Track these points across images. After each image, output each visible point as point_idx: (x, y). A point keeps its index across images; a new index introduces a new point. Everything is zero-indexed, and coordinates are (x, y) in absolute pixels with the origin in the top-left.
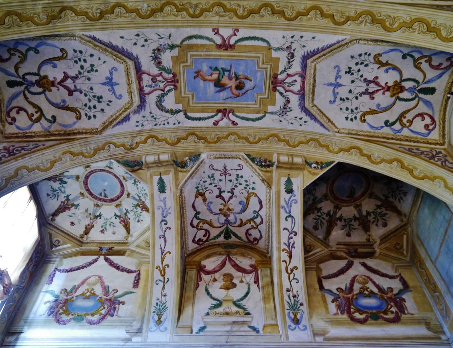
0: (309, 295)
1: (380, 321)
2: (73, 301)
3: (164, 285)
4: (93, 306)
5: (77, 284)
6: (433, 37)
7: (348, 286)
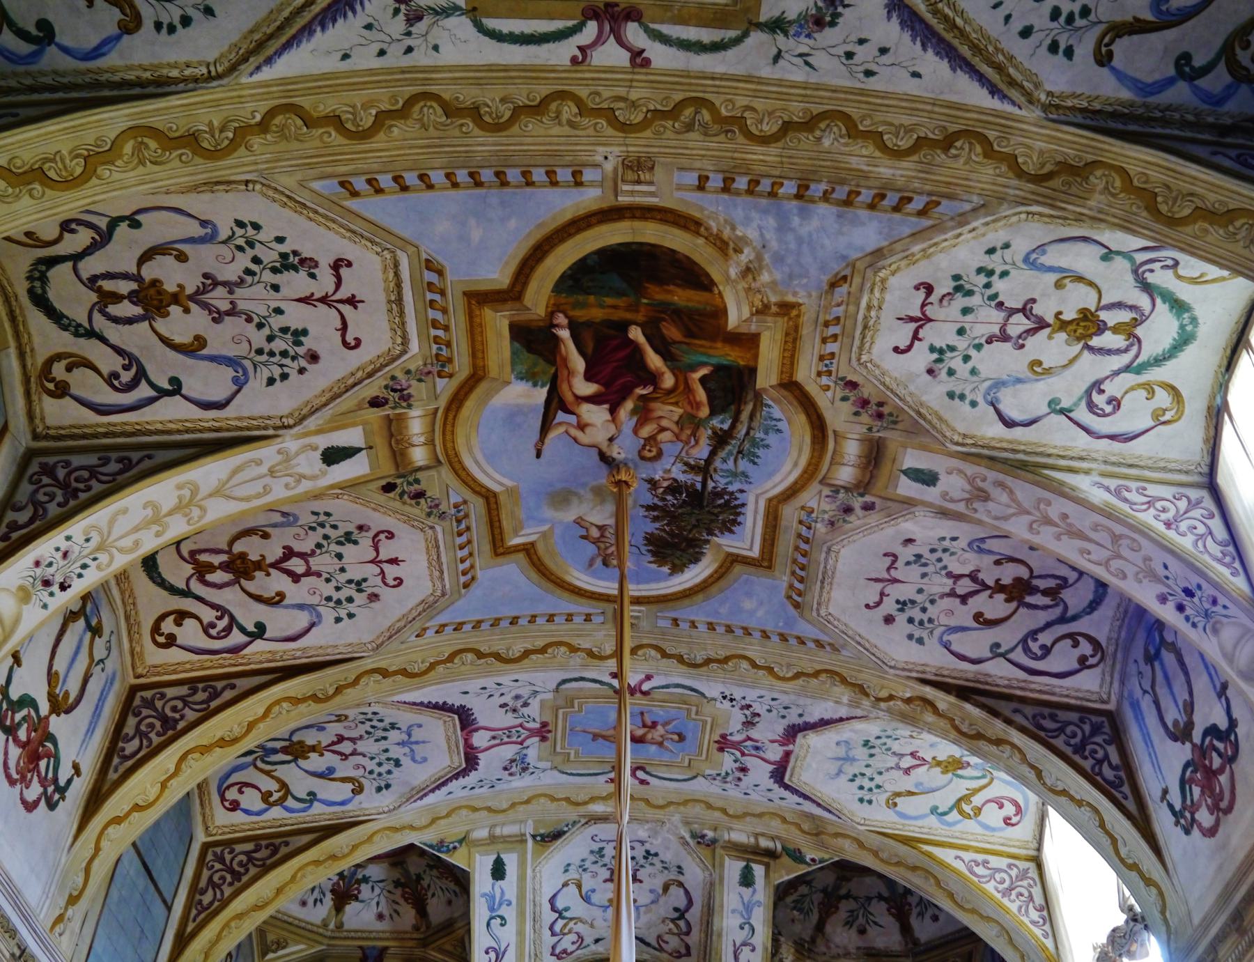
6: (18, 162)
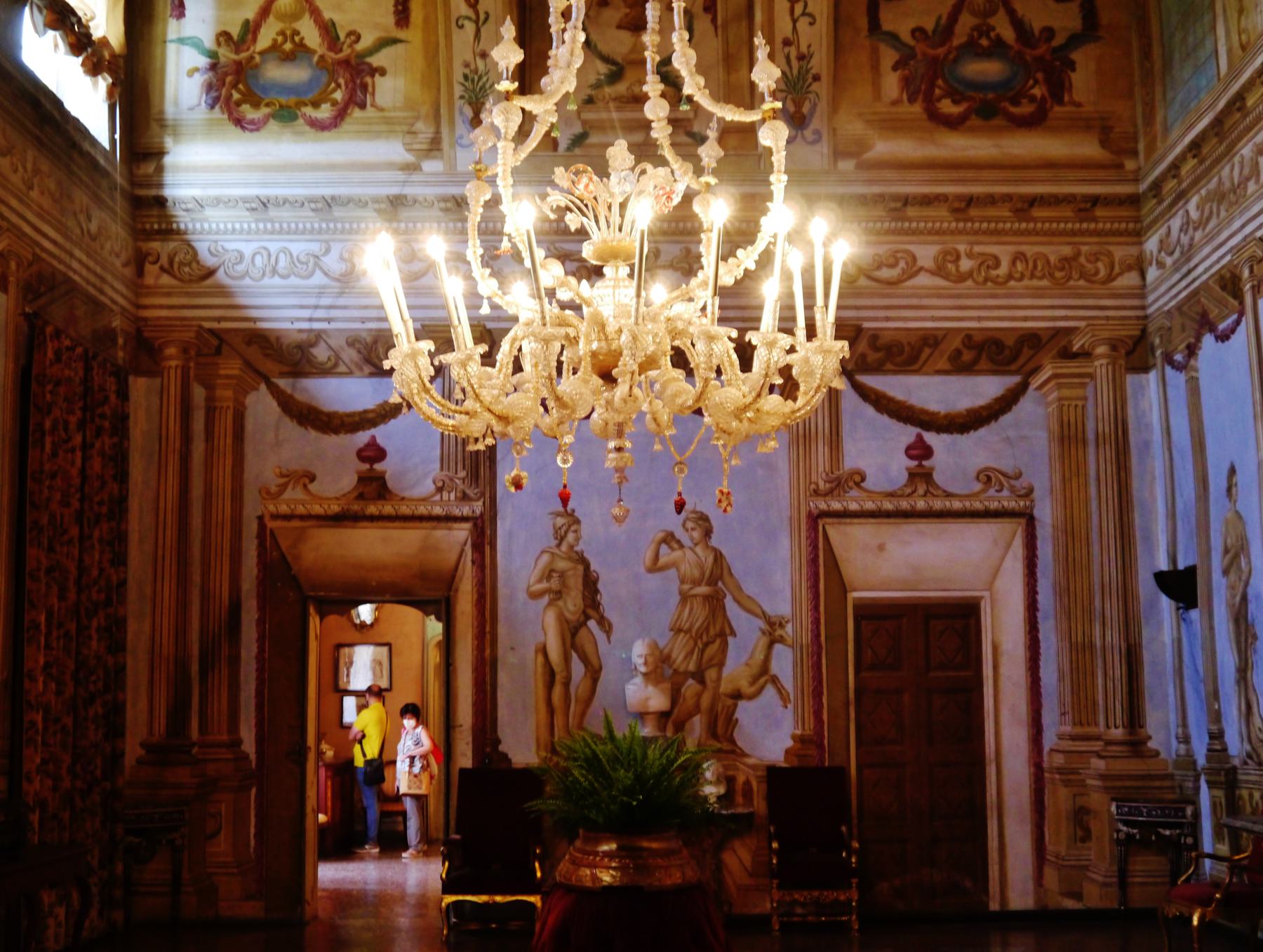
0: (838, 49)
1: (999, 121)
2: (257, 66)
3: (478, 32)
4: (311, 81)
5: (250, 13)
7: (943, 21)
